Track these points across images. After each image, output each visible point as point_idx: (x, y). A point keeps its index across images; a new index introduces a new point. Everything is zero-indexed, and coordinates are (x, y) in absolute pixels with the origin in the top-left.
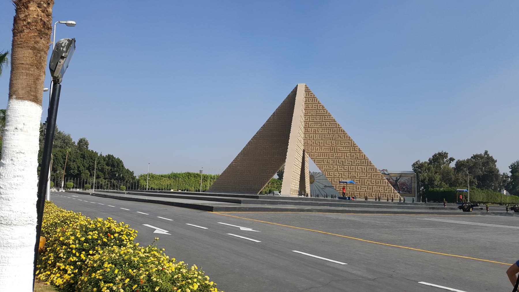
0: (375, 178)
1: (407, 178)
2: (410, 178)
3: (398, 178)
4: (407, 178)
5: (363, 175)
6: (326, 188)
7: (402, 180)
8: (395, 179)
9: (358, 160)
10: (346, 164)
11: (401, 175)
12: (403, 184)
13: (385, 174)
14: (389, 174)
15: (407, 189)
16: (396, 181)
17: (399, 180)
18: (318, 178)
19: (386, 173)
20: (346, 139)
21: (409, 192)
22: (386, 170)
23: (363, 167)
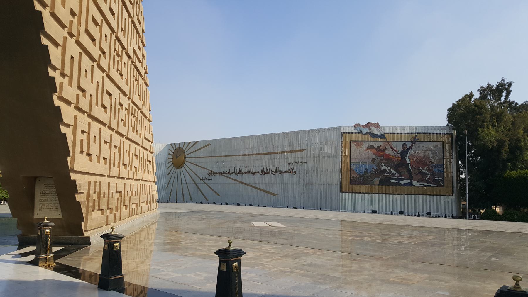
1: (432, 145)
2: (439, 145)
3: (409, 144)
4: (432, 145)
6: (213, 177)
7: (418, 151)
8: (400, 149)
11: (416, 137)
12: (422, 162)
13: (373, 135)
14: (382, 136)
15: (433, 174)
16: (404, 153)
17: (411, 152)
18: (193, 155)
19: (376, 132)
21: (437, 182)
22: (377, 125)
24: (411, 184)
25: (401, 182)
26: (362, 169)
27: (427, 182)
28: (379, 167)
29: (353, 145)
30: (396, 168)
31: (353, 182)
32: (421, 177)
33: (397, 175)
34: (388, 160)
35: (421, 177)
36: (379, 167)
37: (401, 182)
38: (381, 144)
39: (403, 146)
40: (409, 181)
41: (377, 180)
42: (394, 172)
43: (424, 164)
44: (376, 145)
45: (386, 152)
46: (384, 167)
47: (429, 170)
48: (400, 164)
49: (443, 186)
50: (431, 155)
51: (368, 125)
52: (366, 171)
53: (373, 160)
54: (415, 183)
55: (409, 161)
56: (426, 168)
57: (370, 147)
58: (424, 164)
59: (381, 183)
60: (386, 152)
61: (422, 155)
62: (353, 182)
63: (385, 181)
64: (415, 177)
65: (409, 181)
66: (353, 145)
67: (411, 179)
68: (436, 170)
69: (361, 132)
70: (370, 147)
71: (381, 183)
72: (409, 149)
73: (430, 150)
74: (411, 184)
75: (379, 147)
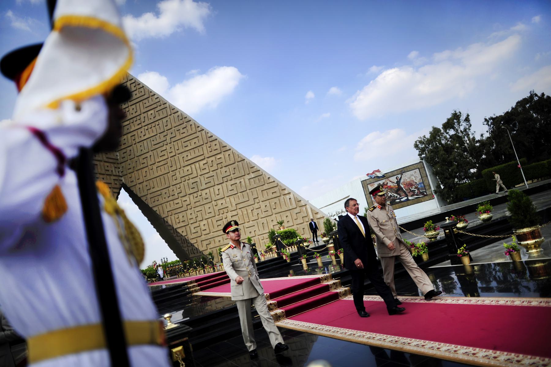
0: (266, 197)
5: (242, 200)
8: (395, 181)
9: (224, 169)
10: (204, 186)
13: (378, 177)
15: (418, 189)
16: (398, 183)
19: (379, 174)
20: (190, 132)
22: (378, 171)
23: (238, 181)
24: (408, 200)
25: (402, 200)
27: (417, 195)
30: (396, 193)
33: (398, 196)
35: (412, 193)
37: (402, 200)
39: (396, 178)
40: (406, 198)
42: (396, 195)
43: (411, 185)
45: (388, 185)
46: (390, 194)
47: (416, 188)
48: (399, 190)
49: (427, 195)
50: (414, 179)
51: (373, 173)
54: (410, 198)
55: (402, 186)
56: (414, 187)
60: (388, 185)
61: (408, 180)
65: (406, 198)
67: (407, 196)
68: (419, 186)
69: (371, 178)
72: (400, 179)
73: (412, 175)
74: (408, 200)
75: (384, 183)
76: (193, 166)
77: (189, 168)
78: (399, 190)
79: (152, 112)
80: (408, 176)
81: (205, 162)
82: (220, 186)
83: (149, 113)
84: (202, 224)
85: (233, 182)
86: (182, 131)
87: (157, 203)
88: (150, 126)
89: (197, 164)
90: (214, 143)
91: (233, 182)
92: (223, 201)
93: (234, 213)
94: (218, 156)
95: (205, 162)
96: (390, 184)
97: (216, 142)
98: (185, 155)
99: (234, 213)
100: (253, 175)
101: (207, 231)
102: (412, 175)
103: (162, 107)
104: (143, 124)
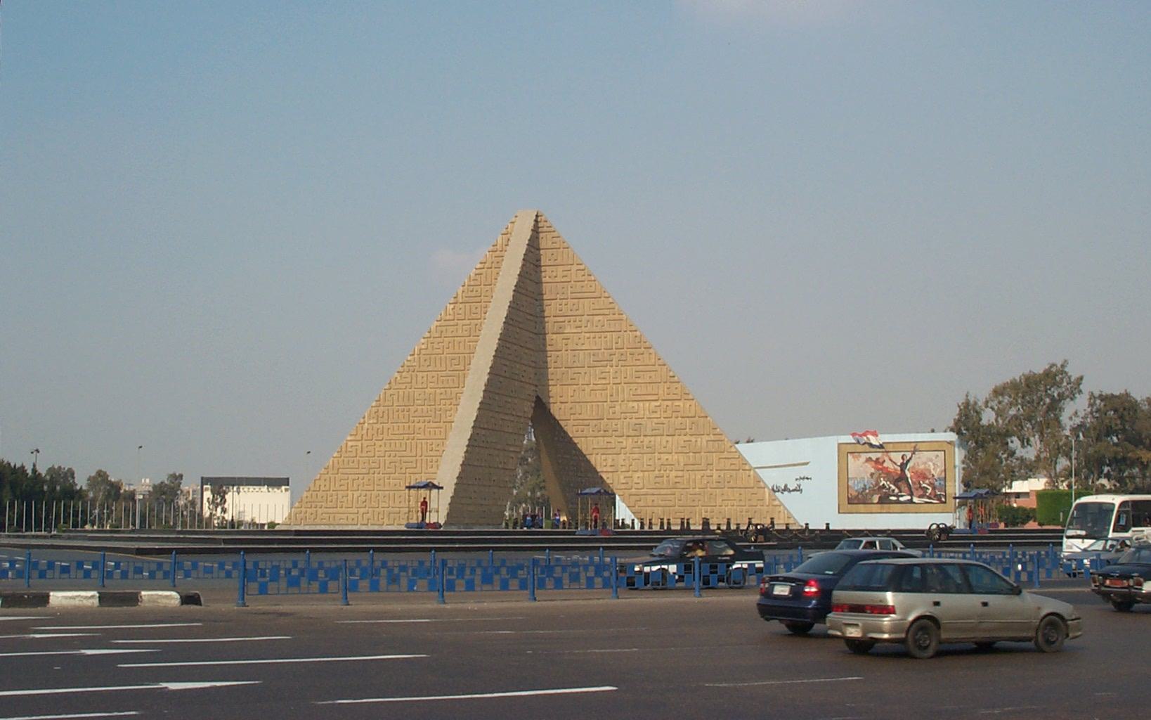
0: (721, 466)
3: (909, 455)
8: (899, 461)
13: (871, 445)
14: (881, 446)
15: (934, 488)
16: (903, 466)
21: (938, 497)
23: (693, 439)
24: (911, 502)
26: (861, 486)
28: (877, 483)
29: (850, 457)
31: (851, 501)
32: (921, 492)
34: (887, 474)
35: (921, 492)
36: (877, 483)
38: (879, 455)
41: (876, 499)
42: (893, 487)
43: (925, 478)
44: (874, 456)
47: (930, 484)
48: (900, 479)
52: (864, 489)
53: (872, 475)
54: (915, 500)
57: (869, 460)
58: (925, 478)
59: (881, 501)
61: (922, 467)
62: (851, 501)
63: (884, 500)
64: (915, 493)
66: (850, 457)
67: (911, 495)
70: (869, 460)
71: (881, 501)
73: (931, 460)
74: (911, 502)
76: (641, 404)
77: (635, 404)
78: (900, 479)
79: (600, 318)
80: (924, 460)
81: (657, 403)
82: (670, 438)
83: (597, 318)
84: (636, 475)
85: (686, 438)
86: (637, 357)
87: (580, 433)
88: (592, 335)
89: (647, 404)
90: (676, 385)
91: (686, 438)
92: (669, 456)
93: (680, 474)
94: (677, 403)
95: (657, 403)
96: (887, 464)
97: (678, 385)
98: (634, 386)
99: (680, 474)
100: (712, 437)
101: (641, 486)
102: (931, 460)
103: (616, 317)
104: (584, 329)
